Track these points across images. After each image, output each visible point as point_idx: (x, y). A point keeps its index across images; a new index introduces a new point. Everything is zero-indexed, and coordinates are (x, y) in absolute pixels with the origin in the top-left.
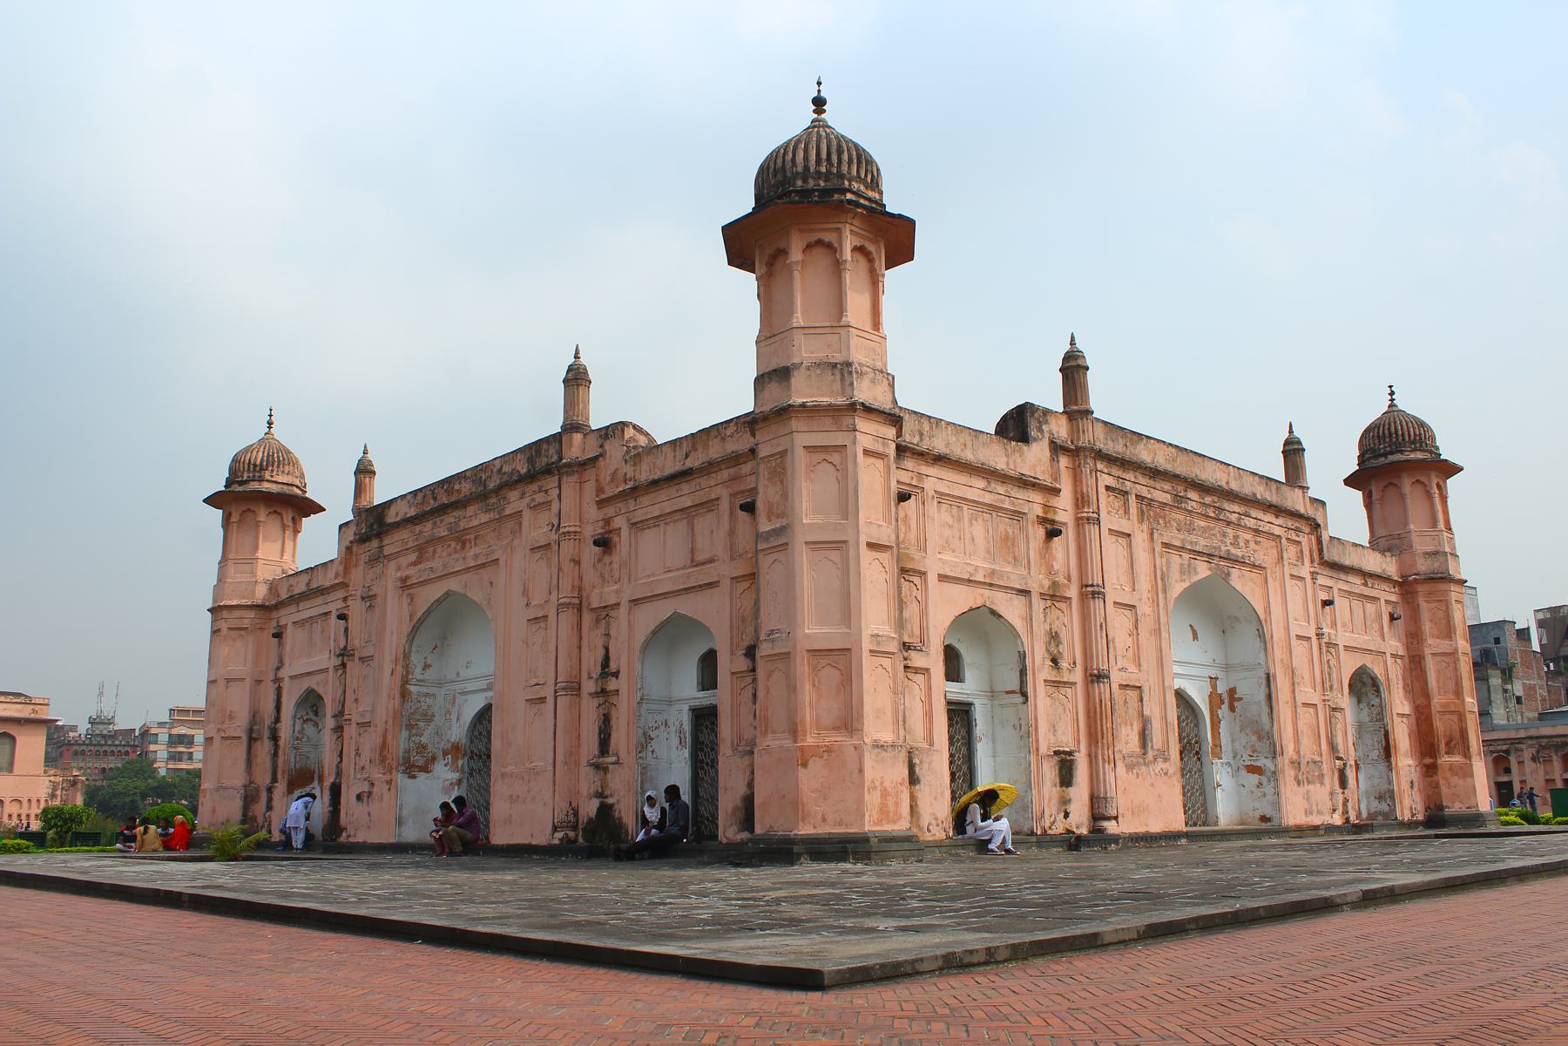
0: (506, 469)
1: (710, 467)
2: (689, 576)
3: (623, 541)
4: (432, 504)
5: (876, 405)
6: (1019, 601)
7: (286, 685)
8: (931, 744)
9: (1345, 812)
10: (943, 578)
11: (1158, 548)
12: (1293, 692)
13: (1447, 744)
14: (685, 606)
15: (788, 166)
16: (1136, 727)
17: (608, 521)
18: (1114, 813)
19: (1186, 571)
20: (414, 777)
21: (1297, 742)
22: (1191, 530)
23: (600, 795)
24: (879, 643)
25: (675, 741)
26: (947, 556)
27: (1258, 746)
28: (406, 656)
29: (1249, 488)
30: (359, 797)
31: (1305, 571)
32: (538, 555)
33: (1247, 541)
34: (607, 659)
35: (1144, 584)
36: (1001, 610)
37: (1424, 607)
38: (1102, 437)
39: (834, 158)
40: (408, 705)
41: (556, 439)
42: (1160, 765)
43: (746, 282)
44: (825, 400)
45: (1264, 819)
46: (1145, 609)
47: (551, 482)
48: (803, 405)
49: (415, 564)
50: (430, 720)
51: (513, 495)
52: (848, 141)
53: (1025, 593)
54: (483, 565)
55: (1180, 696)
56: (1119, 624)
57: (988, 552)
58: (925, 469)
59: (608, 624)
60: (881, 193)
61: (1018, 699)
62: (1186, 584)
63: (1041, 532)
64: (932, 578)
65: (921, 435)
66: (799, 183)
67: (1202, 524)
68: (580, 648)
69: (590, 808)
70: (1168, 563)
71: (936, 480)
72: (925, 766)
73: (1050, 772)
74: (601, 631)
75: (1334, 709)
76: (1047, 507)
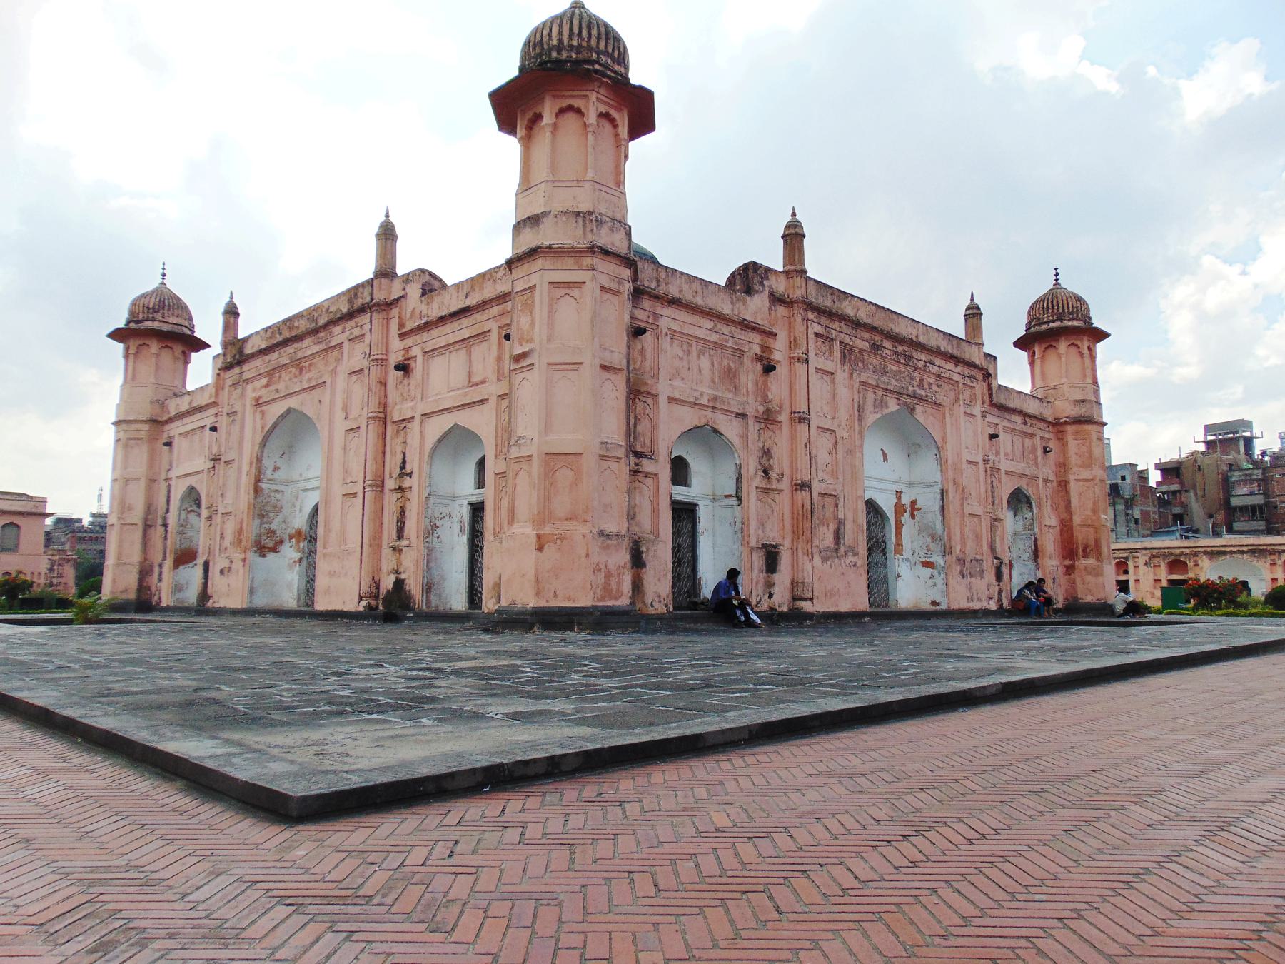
0: (332, 309)
1: (484, 305)
2: (465, 395)
3: (417, 366)
4: (279, 338)
5: (612, 249)
6: (736, 423)
7: (173, 483)
8: (658, 535)
9: (1000, 600)
10: (672, 400)
11: (856, 385)
12: (962, 504)
13: (1084, 550)
14: (463, 418)
15: (545, 39)
16: (832, 527)
17: (407, 350)
18: (809, 595)
19: (879, 405)
20: (264, 556)
21: (963, 543)
22: (884, 371)
23: (397, 572)
24: (607, 449)
25: (456, 529)
26: (678, 383)
27: (932, 546)
28: (259, 460)
29: (934, 341)
30: (222, 572)
31: (977, 410)
32: (354, 378)
33: (930, 385)
34: (404, 462)
35: (843, 414)
36: (722, 429)
37: (1073, 445)
38: (813, 293)
39: (585, 33)
40: (259, 500)
41: (370, 283)
42: (850, 558)
43: (511, 146)
44: (568, 242)
45: (934, 603)
46: (842, 433)
47: (364, 319)
48: (550, 247)
49: (266, 386)
50: (279, 511)
51: (337, 330)
52: (597, 19)
53: (742, 416)
54: (314, 387)
55: (872, 506)
56: (822, 446)
57: (713, 382)
58: (661, 310)
59: (406, 434)
60: (627, 68)
61: (735, 502)
62: (879, 415)
63: (759, 368)
64: (663, 400)
65: (658, 281)
66: (554, 54)
67: (894, 368)
68: (384, 453)
69: (388, 583)
70: (864, 397)
71: (670, 319)
72: (651, 553)
73: (758, 561)
74: (401, 439)
75: (995, 520)
76: (765, 348)
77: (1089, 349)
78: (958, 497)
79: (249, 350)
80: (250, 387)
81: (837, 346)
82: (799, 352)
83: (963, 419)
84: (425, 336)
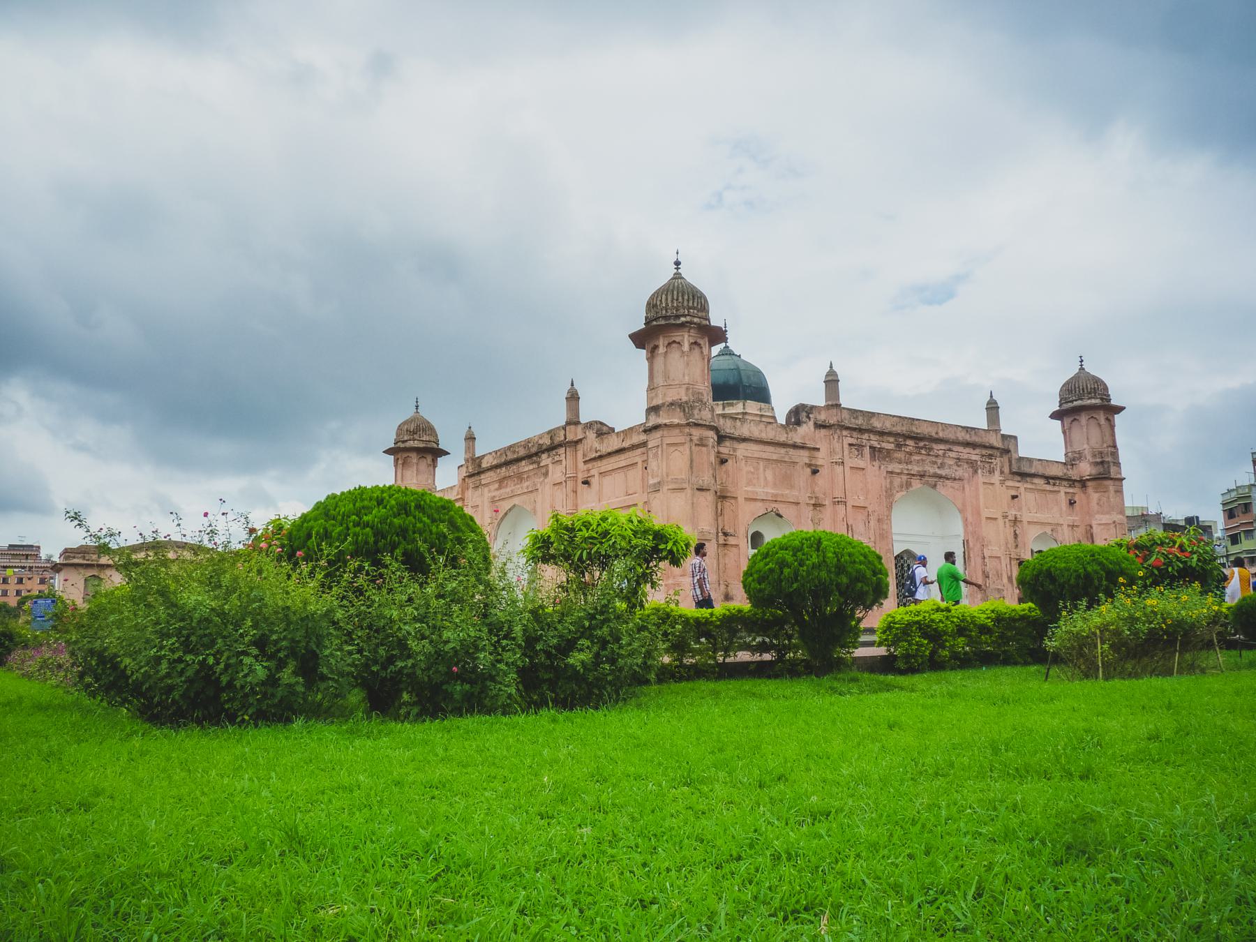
17: (588, 470)
29: (950, 435)
36: (781, 512)
44: (676, 421)
47: (562, 450)
51: (544, 456)
58: (736, 445)
63: (808, 471)
64: (741, 500)
70: (891, 483)
71: (743, 450)
77: (1107, 419)
78: (979, 546)
79: (484, 465)
80: (486, 490)
81: (867, 450)
82: (837, 458)
83: (981, 488)
84: (599, 463)
